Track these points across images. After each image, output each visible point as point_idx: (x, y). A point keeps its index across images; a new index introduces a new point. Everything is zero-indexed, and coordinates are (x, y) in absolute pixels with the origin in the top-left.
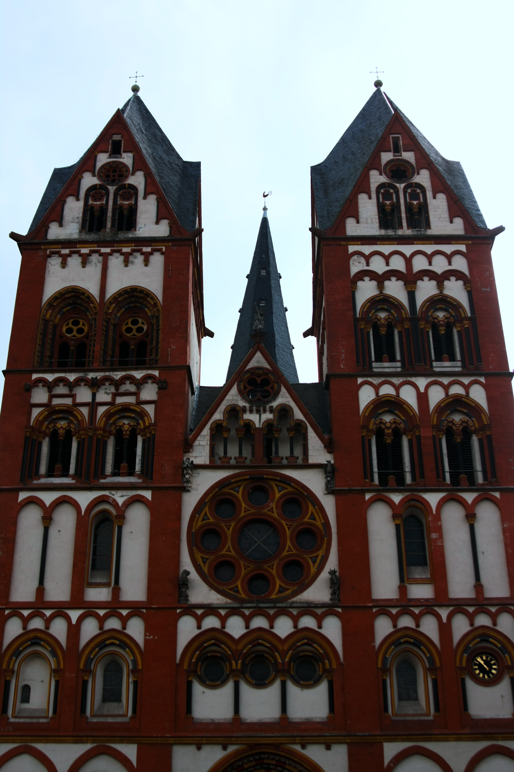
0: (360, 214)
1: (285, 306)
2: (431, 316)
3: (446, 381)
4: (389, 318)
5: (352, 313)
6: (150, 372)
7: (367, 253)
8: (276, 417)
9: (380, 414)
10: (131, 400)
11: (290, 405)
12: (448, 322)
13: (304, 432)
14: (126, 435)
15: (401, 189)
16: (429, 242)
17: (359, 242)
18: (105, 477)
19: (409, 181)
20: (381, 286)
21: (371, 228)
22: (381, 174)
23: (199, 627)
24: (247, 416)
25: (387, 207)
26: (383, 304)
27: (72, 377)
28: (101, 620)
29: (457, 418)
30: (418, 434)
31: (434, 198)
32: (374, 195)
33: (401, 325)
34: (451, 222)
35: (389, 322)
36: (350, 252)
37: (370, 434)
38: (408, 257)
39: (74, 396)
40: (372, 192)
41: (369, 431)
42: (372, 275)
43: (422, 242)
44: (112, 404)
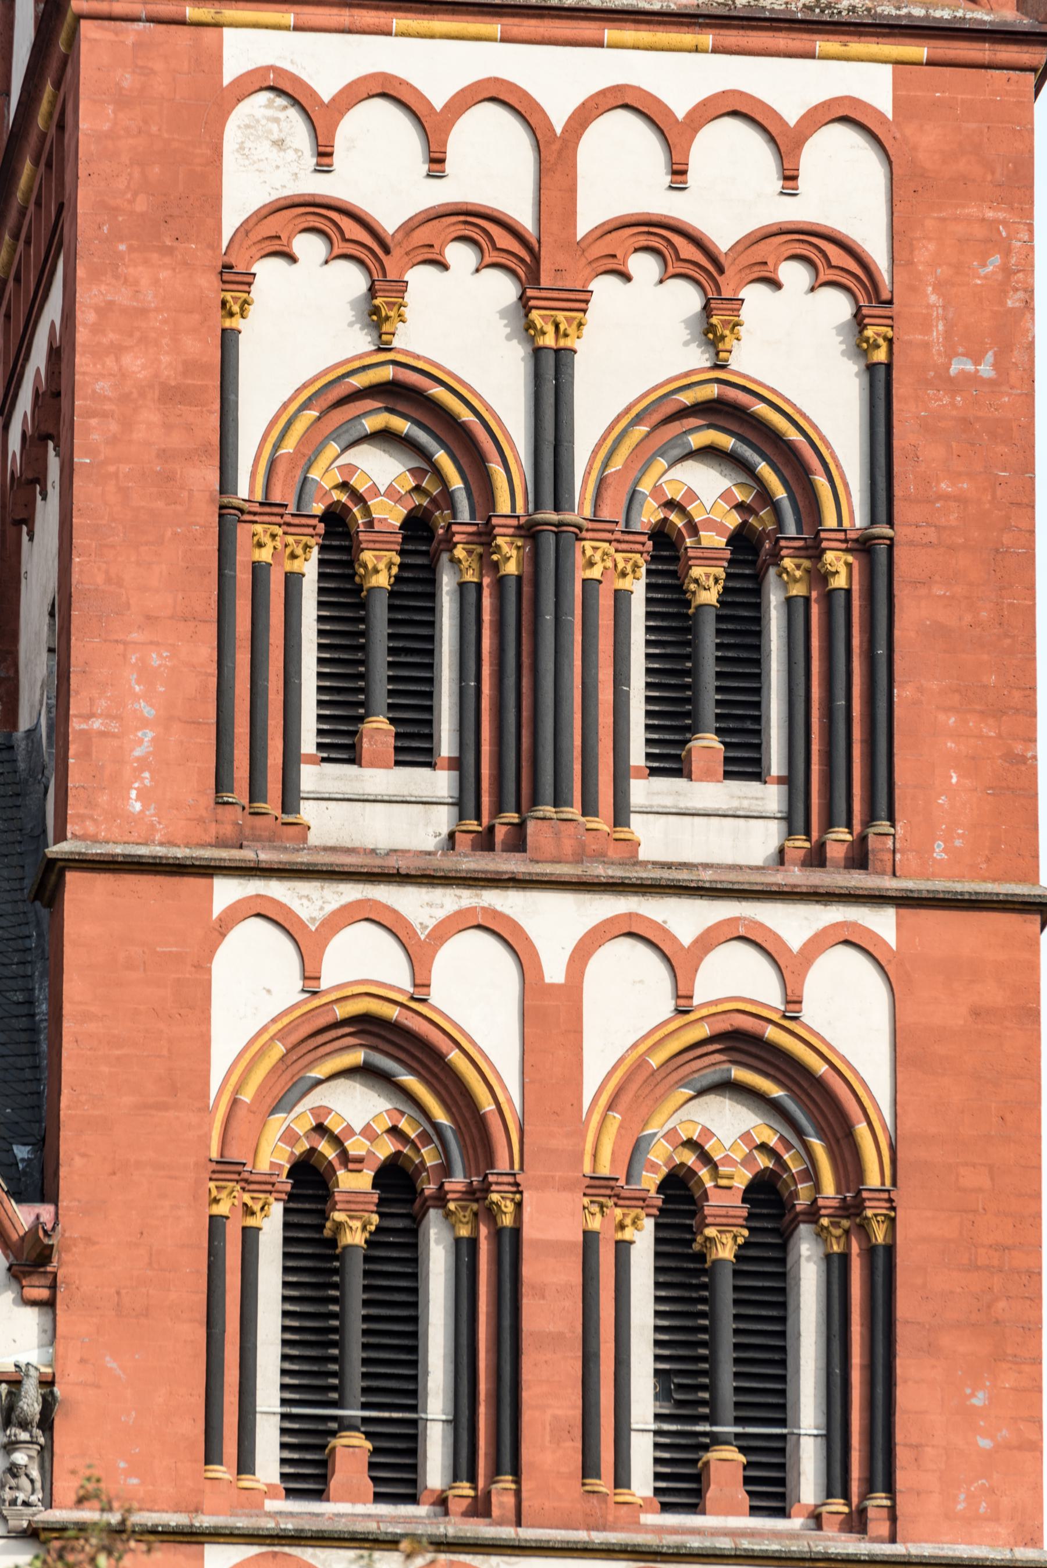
2: (657, 490)
4: (417, 489)
7: (326, 89)
16: (687, 38)
17: (287, 12)
36: (228, 77)
43: (644, 35)
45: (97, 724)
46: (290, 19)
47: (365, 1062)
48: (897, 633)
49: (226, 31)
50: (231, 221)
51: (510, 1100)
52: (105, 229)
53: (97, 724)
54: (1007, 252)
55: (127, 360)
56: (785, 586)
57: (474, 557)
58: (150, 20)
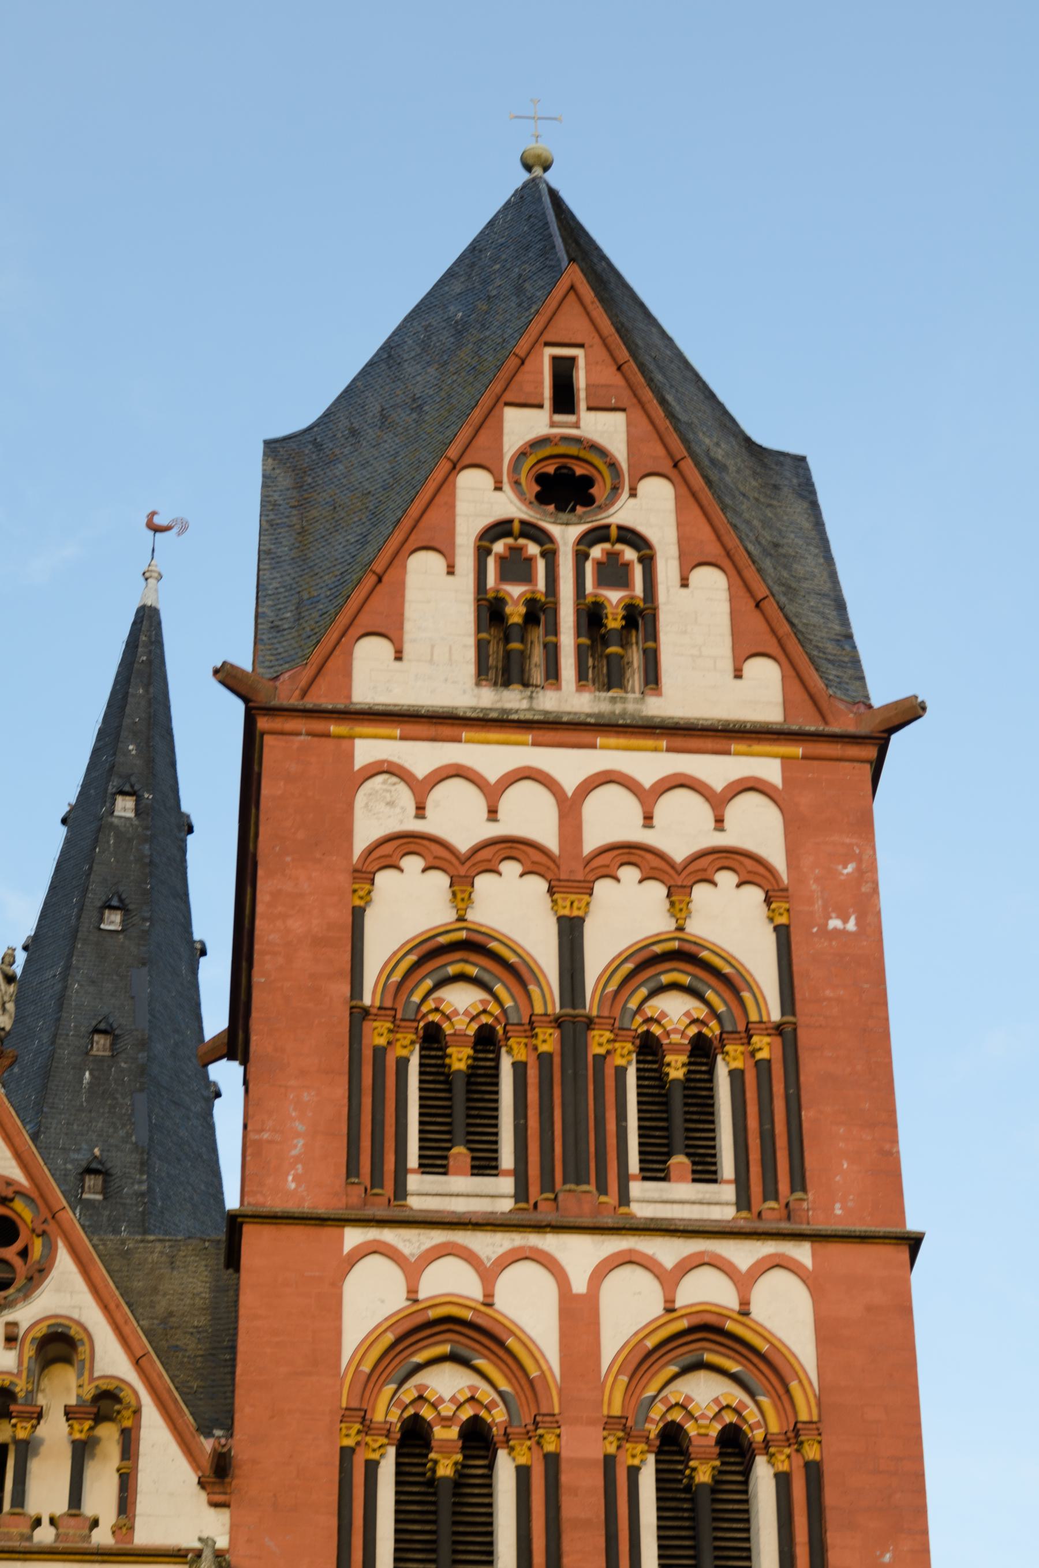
0: (408, 626)
1: (197, 937)
4: (484, 1011)
5: (346, 989)
8: (25, 1365)
9: (419, 1368)
11: (83, 1320)
12: (700, 1034)
13: (127, 1424)
15: (565, 544)
17: (396, 728)
19: (599, 517)
21: (446, 680)
22: (498, 488)
25: (508, 610)
26: (466, 961)
30: (550, 1447)
31: (684, 583)
32: (465, 560)
33: (525, 1040)
34: (738, 675)
35: (483, 1027)
36: (357, 766)
37: (375, 1441)
38: (570, 794)
40: (459, 551)
41: (367, 1427)
43: (622, 741)
45: (266, 1136)
46: (398, 732)
47: (451, 1352)
48: (802, 1078)
49: (359, 743)
51: (550, 1369)
52: (278, 849)
53: (266, 1136)
54: (859, 860)
55: (290, 922)
56: (728, 1064)
57: (522, 1046)
58: (308, 734)
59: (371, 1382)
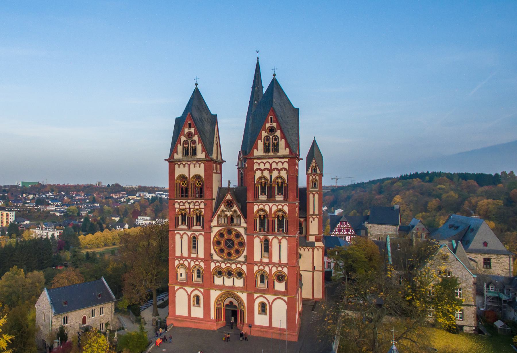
3: (277, 204)
5: (254, 183)
6: (202, 200)
10: (198, 207)
14: (198, 215)
18: (193, 226)
20: (262, 173)
23: (215, 265)
24: (226, 213)
27: (184, 201)
28: (195, 262)
29: (280, 213)
31: (281, 141)
32: (263, 140)
34: (285, 150)
39: (185, 206)
42: (260, 169)
44: (194, 208)
50: (254, 170)
59: (256, 215)
